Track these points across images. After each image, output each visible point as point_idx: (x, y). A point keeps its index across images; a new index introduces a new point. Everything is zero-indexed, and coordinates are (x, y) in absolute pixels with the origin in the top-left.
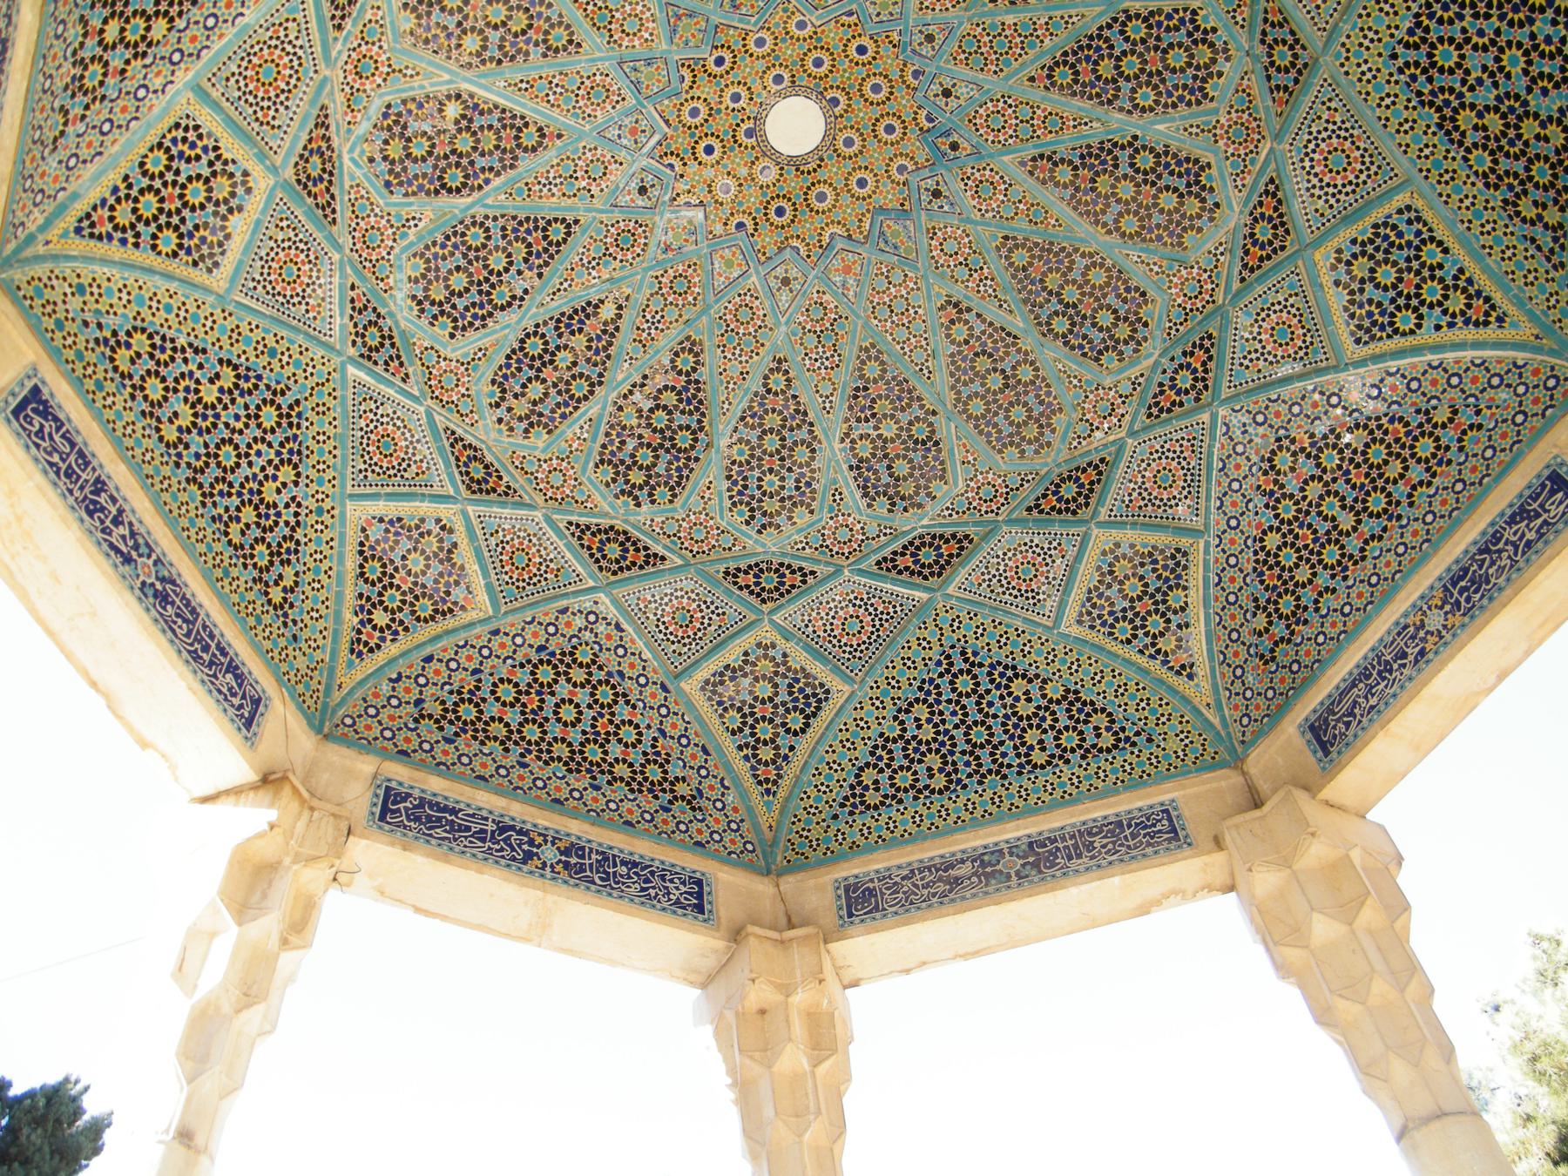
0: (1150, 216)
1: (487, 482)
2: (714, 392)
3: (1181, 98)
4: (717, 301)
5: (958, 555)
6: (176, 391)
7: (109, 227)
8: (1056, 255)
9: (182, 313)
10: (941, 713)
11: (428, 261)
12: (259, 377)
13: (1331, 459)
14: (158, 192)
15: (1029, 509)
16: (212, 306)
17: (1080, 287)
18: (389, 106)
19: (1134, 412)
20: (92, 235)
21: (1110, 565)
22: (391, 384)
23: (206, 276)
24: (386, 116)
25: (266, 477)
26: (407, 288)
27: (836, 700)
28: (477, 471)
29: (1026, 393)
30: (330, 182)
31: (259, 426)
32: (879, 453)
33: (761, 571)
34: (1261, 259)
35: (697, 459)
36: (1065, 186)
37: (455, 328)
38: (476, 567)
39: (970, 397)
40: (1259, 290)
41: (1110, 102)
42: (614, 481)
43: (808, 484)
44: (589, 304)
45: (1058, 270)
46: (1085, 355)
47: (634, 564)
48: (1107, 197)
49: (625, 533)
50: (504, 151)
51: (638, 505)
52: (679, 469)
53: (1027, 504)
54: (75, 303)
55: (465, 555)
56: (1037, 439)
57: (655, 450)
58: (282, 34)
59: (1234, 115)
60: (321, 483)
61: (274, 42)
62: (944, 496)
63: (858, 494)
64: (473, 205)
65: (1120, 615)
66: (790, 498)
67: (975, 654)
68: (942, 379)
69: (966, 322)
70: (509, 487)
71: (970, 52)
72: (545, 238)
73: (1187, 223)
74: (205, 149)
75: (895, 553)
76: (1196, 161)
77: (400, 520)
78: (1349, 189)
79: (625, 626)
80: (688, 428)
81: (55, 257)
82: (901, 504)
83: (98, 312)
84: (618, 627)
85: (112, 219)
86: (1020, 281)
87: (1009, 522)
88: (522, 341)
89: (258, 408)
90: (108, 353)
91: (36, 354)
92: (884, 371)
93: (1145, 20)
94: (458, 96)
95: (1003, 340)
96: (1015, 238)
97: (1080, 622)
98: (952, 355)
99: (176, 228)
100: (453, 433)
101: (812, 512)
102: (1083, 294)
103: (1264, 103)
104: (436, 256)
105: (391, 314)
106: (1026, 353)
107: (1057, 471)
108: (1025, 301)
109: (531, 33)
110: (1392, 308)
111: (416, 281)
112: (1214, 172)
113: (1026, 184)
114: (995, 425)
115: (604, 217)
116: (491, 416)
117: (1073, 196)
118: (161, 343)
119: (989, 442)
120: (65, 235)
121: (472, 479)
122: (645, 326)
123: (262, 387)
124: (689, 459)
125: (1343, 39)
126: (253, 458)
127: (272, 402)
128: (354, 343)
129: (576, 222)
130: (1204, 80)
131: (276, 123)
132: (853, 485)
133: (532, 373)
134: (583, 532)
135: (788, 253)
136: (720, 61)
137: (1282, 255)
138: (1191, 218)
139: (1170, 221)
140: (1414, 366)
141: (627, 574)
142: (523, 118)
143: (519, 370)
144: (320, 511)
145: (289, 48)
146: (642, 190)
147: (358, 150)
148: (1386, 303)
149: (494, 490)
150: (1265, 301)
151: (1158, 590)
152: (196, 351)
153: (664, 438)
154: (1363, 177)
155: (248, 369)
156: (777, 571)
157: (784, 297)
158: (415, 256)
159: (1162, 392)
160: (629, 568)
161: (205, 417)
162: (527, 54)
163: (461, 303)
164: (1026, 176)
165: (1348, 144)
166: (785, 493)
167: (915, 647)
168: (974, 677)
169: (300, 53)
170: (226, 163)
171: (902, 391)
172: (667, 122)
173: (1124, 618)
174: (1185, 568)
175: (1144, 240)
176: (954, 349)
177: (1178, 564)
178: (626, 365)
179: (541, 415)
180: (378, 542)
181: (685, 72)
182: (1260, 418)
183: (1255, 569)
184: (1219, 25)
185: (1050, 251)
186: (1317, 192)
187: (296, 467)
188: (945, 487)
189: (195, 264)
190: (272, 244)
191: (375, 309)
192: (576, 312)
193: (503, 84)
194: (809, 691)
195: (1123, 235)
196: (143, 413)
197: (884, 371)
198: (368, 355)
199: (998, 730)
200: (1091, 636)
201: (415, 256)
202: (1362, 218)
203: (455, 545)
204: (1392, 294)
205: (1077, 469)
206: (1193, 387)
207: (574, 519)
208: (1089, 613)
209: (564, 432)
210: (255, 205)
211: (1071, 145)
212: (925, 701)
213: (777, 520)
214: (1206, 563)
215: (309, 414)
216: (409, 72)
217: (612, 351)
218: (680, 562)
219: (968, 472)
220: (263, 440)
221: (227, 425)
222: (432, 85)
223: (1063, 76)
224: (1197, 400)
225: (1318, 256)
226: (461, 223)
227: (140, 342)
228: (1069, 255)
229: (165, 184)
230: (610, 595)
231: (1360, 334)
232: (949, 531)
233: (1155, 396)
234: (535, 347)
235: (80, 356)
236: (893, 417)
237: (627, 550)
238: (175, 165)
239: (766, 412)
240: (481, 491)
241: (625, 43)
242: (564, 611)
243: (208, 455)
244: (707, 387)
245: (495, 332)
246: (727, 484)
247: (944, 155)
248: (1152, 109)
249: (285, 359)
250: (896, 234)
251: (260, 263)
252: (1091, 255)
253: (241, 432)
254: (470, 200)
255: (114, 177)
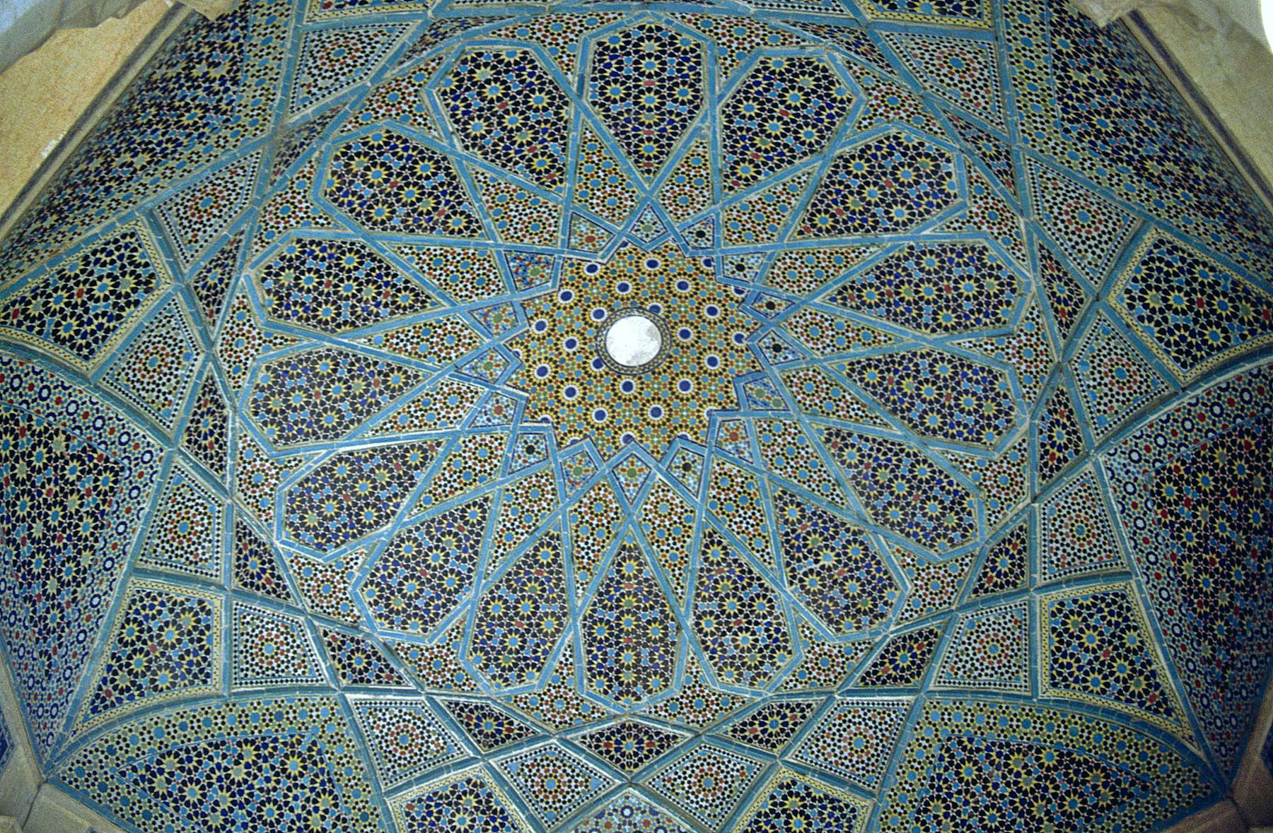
0: (960, 306)
1: (500, 732)
2: (665, 581)
3: (930, 204)
4: (636, 506)
5: (929, 651)
6: (210, 785)
7: (116, 694)
8: (900, 364)
9: (195, 724)
10: (955, 805)
11: (378, 584)
12: (276, 740)
13: (1206, 482)
14: (142, 649)
15: (976, 591)
16: (218, 707)
17: (934, 383)
18: (291, 494)
19: (1031, 480)
20: (106, 707)
21: (1064, 623)
22: (389, 691)
23: (203, 687)
24: (292, 501)
25: (309, 813)
26: (370, 611)
27: (864, 815)
28: (489, 726)
29: (931, 488)
30: (273, 568)
31: (288, 777)
32: (828, 582)
33: (765, 718)
34: (1070, 314)
35: (673, 643)
36: (877, 305)
37: (425, 623)
38: (514, 806)
39: (885, 508)
40: (1081, 341)
41: (874, 228)
42: (610, 687)
43: (777, 631)
44: (527, 556)
45: (908, 376)
46: (966, 439)
47: (650, 751)
48: (916, 303)
49: (636, 726)
50: (399, 477)
51: (639, 699)
52: (661, 657)
53: (972, 587)
54: (111, 763)
55: (502, 799)
56: (959, 525)
57: (634, 649)
58: (179, 499)
59: (981, 203)
60: (357, 796)
61: (177, 507)
62: (900, 598)
63: (824, 625)
64: (394, 528)
65: (1088, 668)
66: (767, 647)
67: (970, 740)
68: (854, 501)
69: (853, 446)
70: (521, 729)
71: (737, 231)
72: (466, 523)
73: (994, 301)
74: (162, 604)
75: (875, 665)
76: (973, 249)
77: (435, 794)
78: (1105, 237)
79: (659, 808)
80: (655, 620)
81: (84, 739)
82: (865, 619)
83: (131, 759)
84: (653, 812)
85: (115, 688)
86: (882, 395)
87: (962, 608)
88: (485, 609)
89: (283, 763)
90: (147, 785)
91: (91, 821)
92: (803, 510)
93: (861, 157)
94: (340, 460)
95: (890, 450)
96: (859, 362)
97: (1055, 685)
98: (854, 477)
99: (167, 666)
100: (457, 704)
101: (790, 653)
102: (939, 388)
103: (998, 188)
104: (383, 577)
105: (368, 635)
106: (915, 455)
107: (988, 547)
108: (894, 411)
109: (372, 389)
110: (1198, 328)
111: (376, 603)
112: (992, 252)
113: (843, 315)
114: (918, 525)
115: (507, 485)
116: (485, 678)
117: (888, 311)
118: (186, 756)
119: (919, 541)
120: (86, 718)
121: (487, 736)
122: (583, 553)
123: (280, 746)
124: (666, 645)
125: (1020, 127)
126: (292, 804)
127: (293, 754)
128: (344, 675)
129: (486, 500)
130: (939, 184)
131: (207, 556)
132: (816, 618)
133: (504, 630)
134: (598, 740)
135: (679, 444)
136: (541, 326)
137: (1084, 307)
138: (996, 296)
139: (980, 304)
140: (1239, 378)
141: (647, 763)
142: (400, 447)
143: (492, 631)
144: (365, 817)
145: (190, 504)
146: (530, 450)
147: (284, 534)
148: (1191, 325)
149: (508, 737)
150: (1092, 350)
151: (1113, 635)
152: (217, 747)
153: (638, 637)
154: (1110, 225)
155: (263, 739)
156: (779, 713)
157: (691, 480)
158: (366, 586)
159: (1046, 452)
160: (647, 757)
161: (241, 793)
162: (378, 403)
163: (420, 603)
164: (842, 309)
165: (1082, 202)
166: (760, 645)
167: (916, 748)
168: (976, 763)
169: (200, 501)
170: (182, 603)
171: (825, 522)
172: (523, 390)
173: (1093, 670)
174: (1129, 609)
175: (966, 327)
176: (853, 471)
177: (1121, 607)
178: (580, 591)
179: (525, 659)
180: (424, 818)
181: (516, 349)
182: (1135, 456)
183: (1184, 599)
184: (924, 139)
185: (893, 362)
186: (1081, 247)
187: (331, 792)
188: (897, 593)
189: (192, 683)
190: (245, 637)
191: (352, 640)
192: (519, 567)
193: (370, 433)
194: (837, 814)
195: (946, 329)
196: (190, 817)
197: (803, 510)
198: (360, 680)
199: (1007, 809)
200: (1068, 695)
201: (366, 586)
202: (1125, 264)
203: (490, 795)
204: (1191, 315)
205: (1004, 541)
206: (1070, 441)
207: (586, 732)
208: (1060, 674)
209: (551, 665)
210: (220, 623)
211: (863, 271)
212: (938, 797)
213: (763, 669)
214: (1144, 600)
215: (327, 746)
216: (293, 463)
217: (563, 585)
218: (689, 735)
219: (910, 572)
220: (296, 786)
221: (261, 790)
222: (315, 463)
223: (823, 221)
224: (1077, 452)
225: (1112, 301)
226: (392, 544)
227: (170, 763)
228: (910, 360)
229: (145, 642)
230: (636, 786)
231: (1182, 358)
232: (916, 629)
233: (1042, 458)
234: (497, 609)
235: (125, 801)
236: (826, 547)
237: (641, 741)
238: (145, 626)
239: (716, 582)
240: (496, 742)
241: (453, 355)
242: (601, 815)
243: (253, 820)
244: (658, 581)
245: (459, 611)
246: (706, 655)
247: (766, 315)
248: (911, 221)
249: (291, 715)
250: (760, 393)
251: (242, 656)
252: (929, 355)
253: (275, 789)
254: (390, 525)
255: (105, 660)
